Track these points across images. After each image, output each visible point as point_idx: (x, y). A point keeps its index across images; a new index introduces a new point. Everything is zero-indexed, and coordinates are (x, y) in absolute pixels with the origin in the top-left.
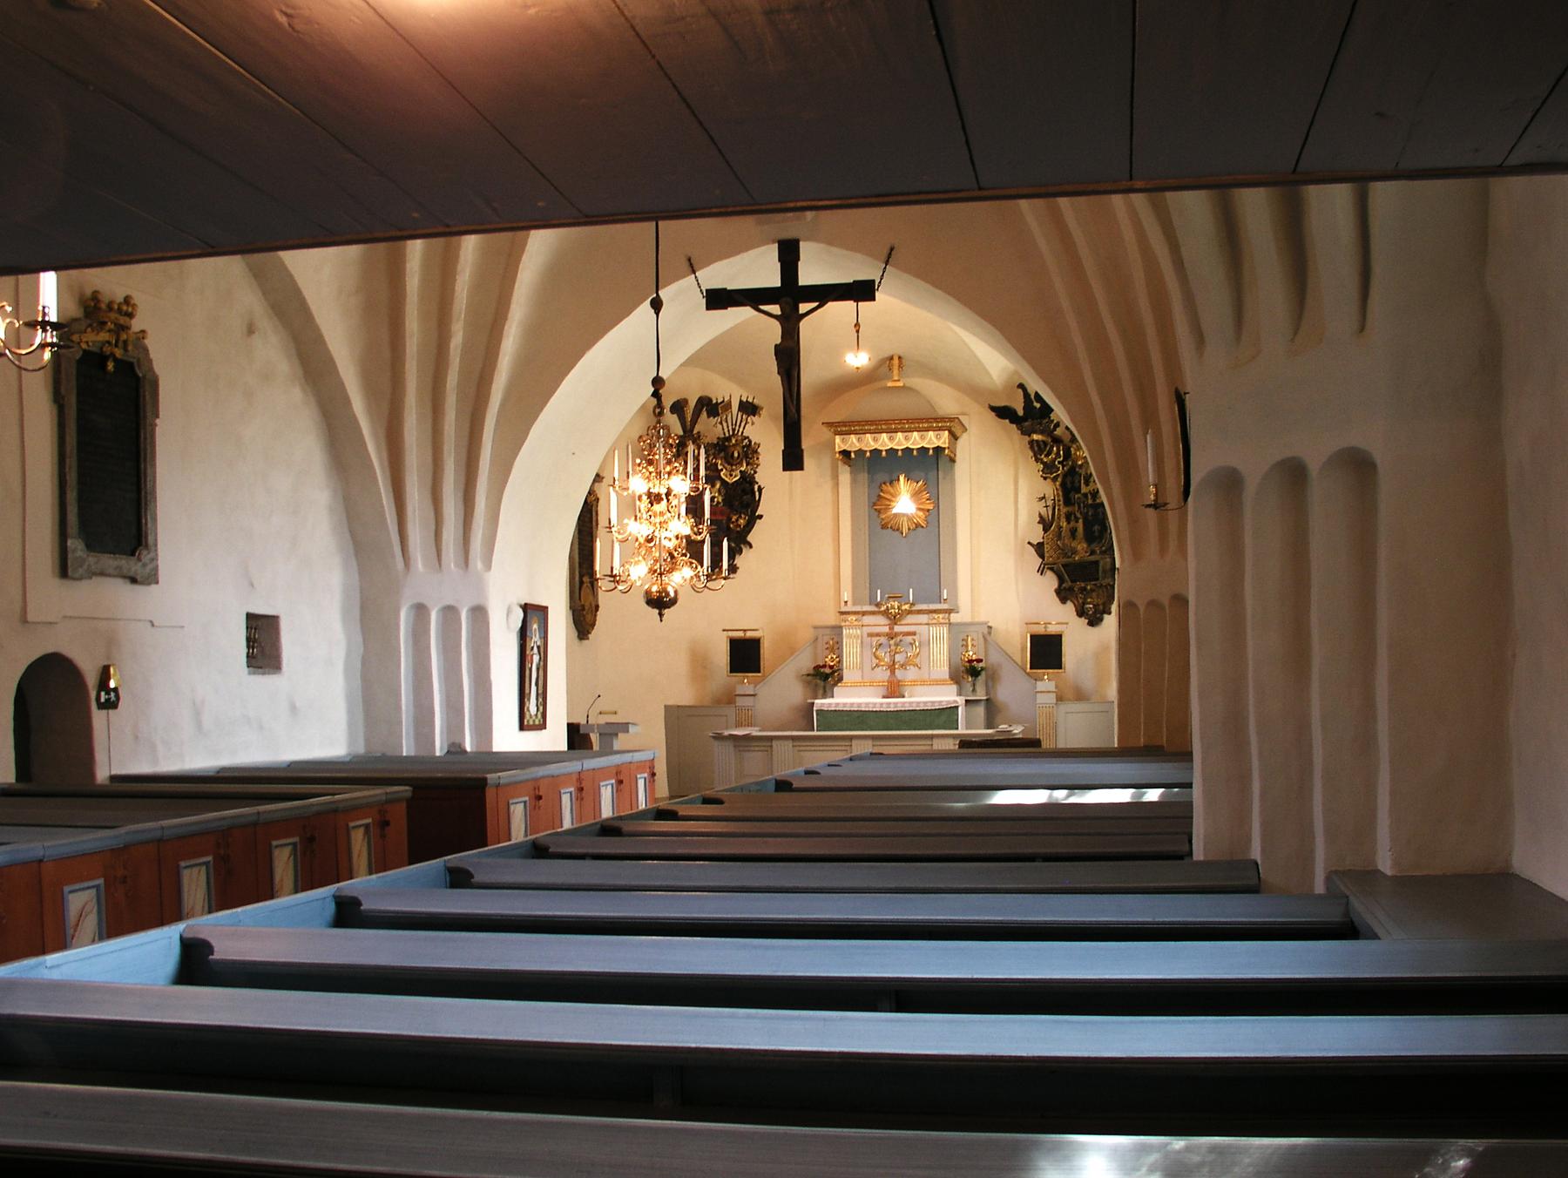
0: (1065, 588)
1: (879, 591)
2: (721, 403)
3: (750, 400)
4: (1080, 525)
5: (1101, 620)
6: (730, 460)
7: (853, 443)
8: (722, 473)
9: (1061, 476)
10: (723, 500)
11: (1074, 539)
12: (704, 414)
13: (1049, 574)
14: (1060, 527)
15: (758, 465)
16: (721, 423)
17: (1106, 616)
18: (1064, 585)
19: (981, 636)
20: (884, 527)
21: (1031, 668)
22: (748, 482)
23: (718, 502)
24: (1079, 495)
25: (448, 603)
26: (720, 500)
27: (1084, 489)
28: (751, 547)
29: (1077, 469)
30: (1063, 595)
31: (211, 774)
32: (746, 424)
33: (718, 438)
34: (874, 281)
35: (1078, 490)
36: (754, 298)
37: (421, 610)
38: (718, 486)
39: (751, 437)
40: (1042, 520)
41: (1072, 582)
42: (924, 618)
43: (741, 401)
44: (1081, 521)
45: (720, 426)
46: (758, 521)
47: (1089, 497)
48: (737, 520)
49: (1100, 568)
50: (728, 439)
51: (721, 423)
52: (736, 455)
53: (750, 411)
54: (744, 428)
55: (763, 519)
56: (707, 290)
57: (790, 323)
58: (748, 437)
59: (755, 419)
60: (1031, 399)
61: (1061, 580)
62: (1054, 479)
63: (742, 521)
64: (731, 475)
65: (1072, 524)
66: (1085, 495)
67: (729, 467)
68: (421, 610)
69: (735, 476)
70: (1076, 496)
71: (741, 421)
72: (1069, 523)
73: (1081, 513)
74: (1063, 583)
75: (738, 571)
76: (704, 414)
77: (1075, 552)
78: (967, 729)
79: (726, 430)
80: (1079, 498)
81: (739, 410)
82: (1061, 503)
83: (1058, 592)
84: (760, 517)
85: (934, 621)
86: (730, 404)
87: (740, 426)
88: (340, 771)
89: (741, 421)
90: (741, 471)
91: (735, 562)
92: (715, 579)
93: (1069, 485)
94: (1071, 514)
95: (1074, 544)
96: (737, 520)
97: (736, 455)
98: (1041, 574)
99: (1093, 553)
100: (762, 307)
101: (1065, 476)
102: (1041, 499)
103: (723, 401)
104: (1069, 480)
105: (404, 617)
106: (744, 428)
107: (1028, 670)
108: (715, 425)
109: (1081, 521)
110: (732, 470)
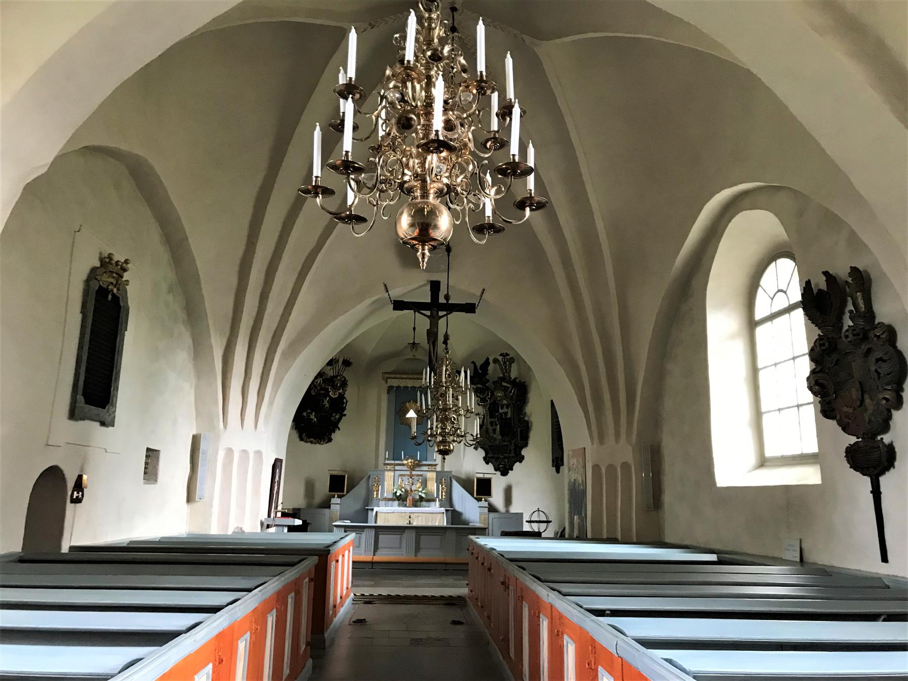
1: (403, 452)
3: (348, 359)
5: (508, 472)
6: (335, 388)
7: (395, 383)
9: (488, 405)
10: (329, 406)
11: (494, 434)
13: (479, 449)
15: (346, 390)
16: (333, 369)
17: (510, 471)
18: (489, 456)
19: (449, 478)
20: (402, 424)
21: (477, 495)
22: (342, 397)
23: (327, 407)
25: (244, 449)
27: (501, 411)
28: (339, 429)
29: (497, 402)
30: (487, 460)
31: (124, 545)
33: (331, 376)
34: (475, 304)
35: (498, 411)
36: (417, 307)
37: (230, 451)
38: (328, 399)
42: (425, 468)
43: (344, 360)
44: (498, 425)
45: (332, 371)
47: (503, 415)
48: (335, 416)
50: (336, 377)
51: (333, 369)
52: (339, 385)
55: (346, 416)
56: (394, 301)
57: (434, 320)
58: (344, 377)
60: (477, 369)
61: (487, 454)
62: (484, 406)
63: (337, 417)
64: (334, 394)
65: (494, 427)
66: (501, 414)
68: (230, 451)
70: (497, 414)
72: (492, 426)
74: (488, 454)
75: (332, 441)
77: (496, 439)
78: (452, 525)
79: (335, 372)
81: (342, 364)
82: (488, 417)
83: (485, 459)
84: (345, 415)
85: (430, 470)
86: (338, 361)
88: (230, 544)
92: (322, 444)
95: (495, 436)
96: (335, 416)
97: (339, 385)
99: (504, 441)
100: (421, 311)
103: (336, 359)
105: (221, 455)
107: (475, 496)
108: (330, 370)
109: (498, 425)
110: (335, 392)
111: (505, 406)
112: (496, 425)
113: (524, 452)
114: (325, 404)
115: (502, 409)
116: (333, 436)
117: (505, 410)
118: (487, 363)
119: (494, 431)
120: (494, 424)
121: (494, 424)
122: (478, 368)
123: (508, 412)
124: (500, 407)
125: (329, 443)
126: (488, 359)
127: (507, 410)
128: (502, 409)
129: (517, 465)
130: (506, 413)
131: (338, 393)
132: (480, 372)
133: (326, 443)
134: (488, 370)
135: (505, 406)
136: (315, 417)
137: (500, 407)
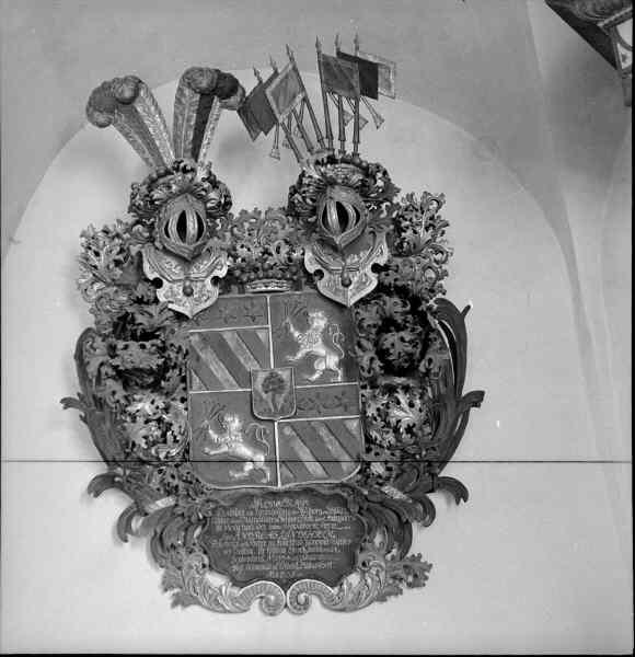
2: (271, 80)
3: (348, 50)
8: (321, 284)
10: (341, 363)
12: (227, 120)
26: (332, 361)
32: (357, 129)
39: (385, 166)
46: (473, 410)
48: (383, 414)
51: (291, 145)
52: (333, 216)
53: (355, 80)
54: (356, 142)
59: (382, 104)
67: (335, 265)
69: (362, 284)
71: (343, 123)
76: (227, 120)
84: (477, 398)
87: (342, 139)
89: (343, 123)
90: (376, 268)
91: (413, 551)
103: (276, 74)
106: (356, 142)
114: (311, 358)
116: (423, 541)
125: (409, 593)
131: (368, 270)
133: (382, 598)
136: (253, 440)
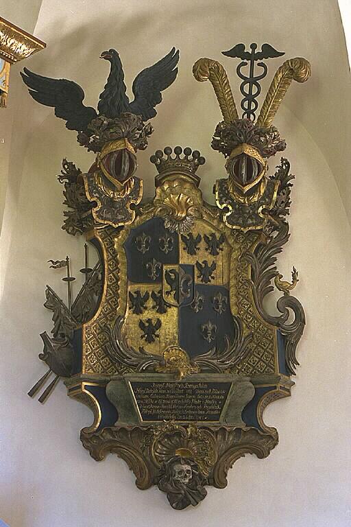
0: (123, 429)
4: (170, 321)
5: (203, 496)
11: (150, 340)
14: (113, 317)
17: (211, 490)
24: (175, 267)
27: (185, 259)
40: (52, 300)
41: (145, 417)
47: (196, 272)
49: (227, 402)
65: (147, 315)
66: (189, 269)
72: (138, 311)
73: (176, 297)
80: (172, 271)
93: (143, 249)
94: (146, 298)
95: (150, 349)
98: (42, 400)
101: (136, 232)
102: (57, 265)
104: (144, 239)
109: (173, 312)
111: (202, 245)
112: (162, 308)
113: (271, 416)
115: (192, 251)
117: (203, 255)
118: (163, 72)
119: (150, 331)
120: (150, 303)
121: (150, 303)
122: (129, 82)
123: (214, 266)
124: (182, 246)
126: (173, 58)
127: (210, 259)
128: (192, 250)
129: (244, 469)
130: (206, 270)
132: (131, 98)
134: (159, 100)
135: (202, 245)
137: (182, 246)
